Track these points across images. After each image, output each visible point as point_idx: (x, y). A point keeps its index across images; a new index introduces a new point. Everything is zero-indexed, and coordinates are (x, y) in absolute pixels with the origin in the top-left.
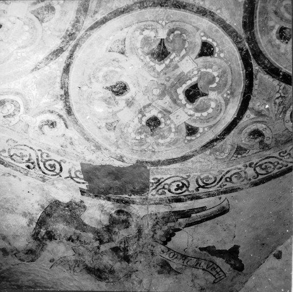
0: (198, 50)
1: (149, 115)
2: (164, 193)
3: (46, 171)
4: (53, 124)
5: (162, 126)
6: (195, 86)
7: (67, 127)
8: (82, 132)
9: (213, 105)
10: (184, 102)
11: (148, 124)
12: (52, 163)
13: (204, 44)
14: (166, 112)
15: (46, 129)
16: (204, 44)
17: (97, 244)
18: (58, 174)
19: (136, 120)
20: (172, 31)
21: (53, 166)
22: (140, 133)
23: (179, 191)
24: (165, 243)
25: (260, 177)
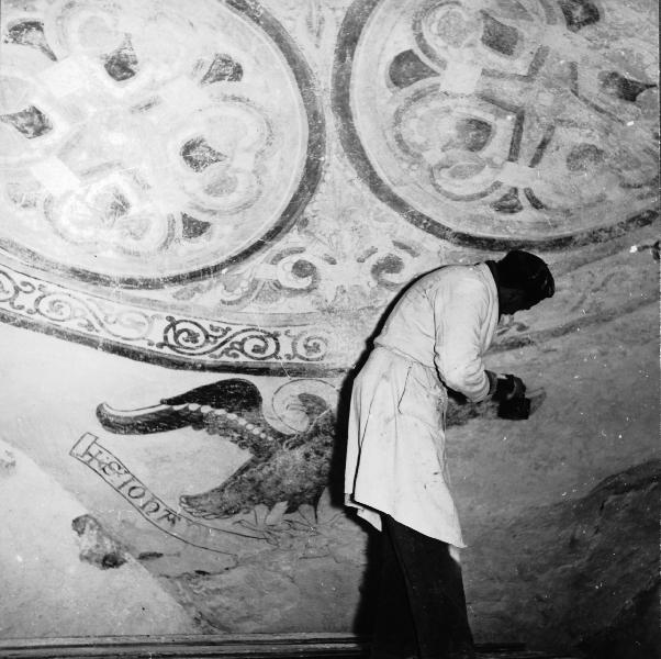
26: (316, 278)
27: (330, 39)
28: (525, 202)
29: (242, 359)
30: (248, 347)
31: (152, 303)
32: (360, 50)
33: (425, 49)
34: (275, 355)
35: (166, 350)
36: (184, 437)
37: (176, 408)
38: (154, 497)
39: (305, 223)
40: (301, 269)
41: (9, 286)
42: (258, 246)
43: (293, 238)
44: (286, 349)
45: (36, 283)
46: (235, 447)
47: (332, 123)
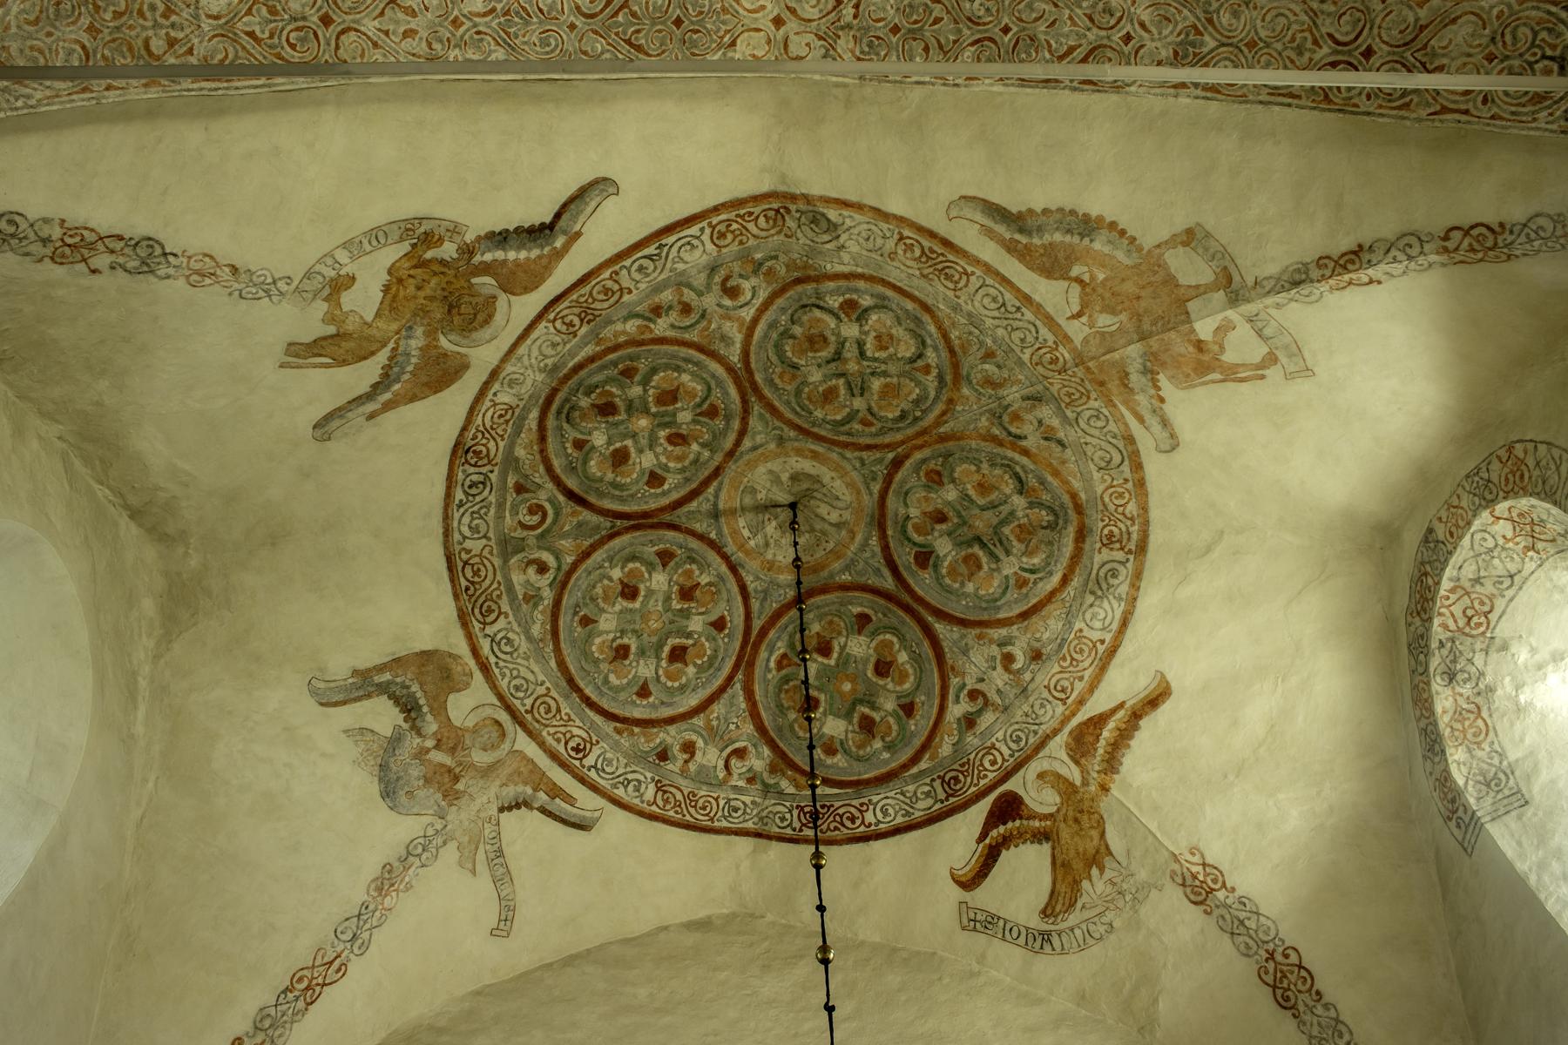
0: (713, 617)
1: (626, 641)
2: (558, 741)
3: (477, 611)
4: (542, 568)
5: (627, 662)
6: (684, 649)
7: (550, 585)
8: (557, 603)
9: (684, 680)
10: (664, 655)
11: (617, 650)
12: (494, 607)
13: (722, 618)
14: (642, 653)
15: (531, 571)
16: (722, 618)
17: (430, 743)
18: (485, 624)
19: (611, 636)
20: (710, 584)
21: (490, 611)
22: (602, 652)
23: (573, 754)
24: (501, 810)
25: (654, 808)
26: (984, 695)
27: (886, 572)
28: (1027, 575)
29: (991, 776)
30: (987, 765)
31: (922, 773)
32: (901, 569)
33: (920, 546)
34: (1004, 760)
35: (952, 800)
36: (1006, 856)
37: (987, 841)
38: (1027, 929)
39: (953, 668)
40: (973, 695)
41: (857, 814)
42: (944, 697)
43: (955, 681)
44: (1006, 752)
45: (865, 800)
46: (1036, 846)
47: (907, 599)
